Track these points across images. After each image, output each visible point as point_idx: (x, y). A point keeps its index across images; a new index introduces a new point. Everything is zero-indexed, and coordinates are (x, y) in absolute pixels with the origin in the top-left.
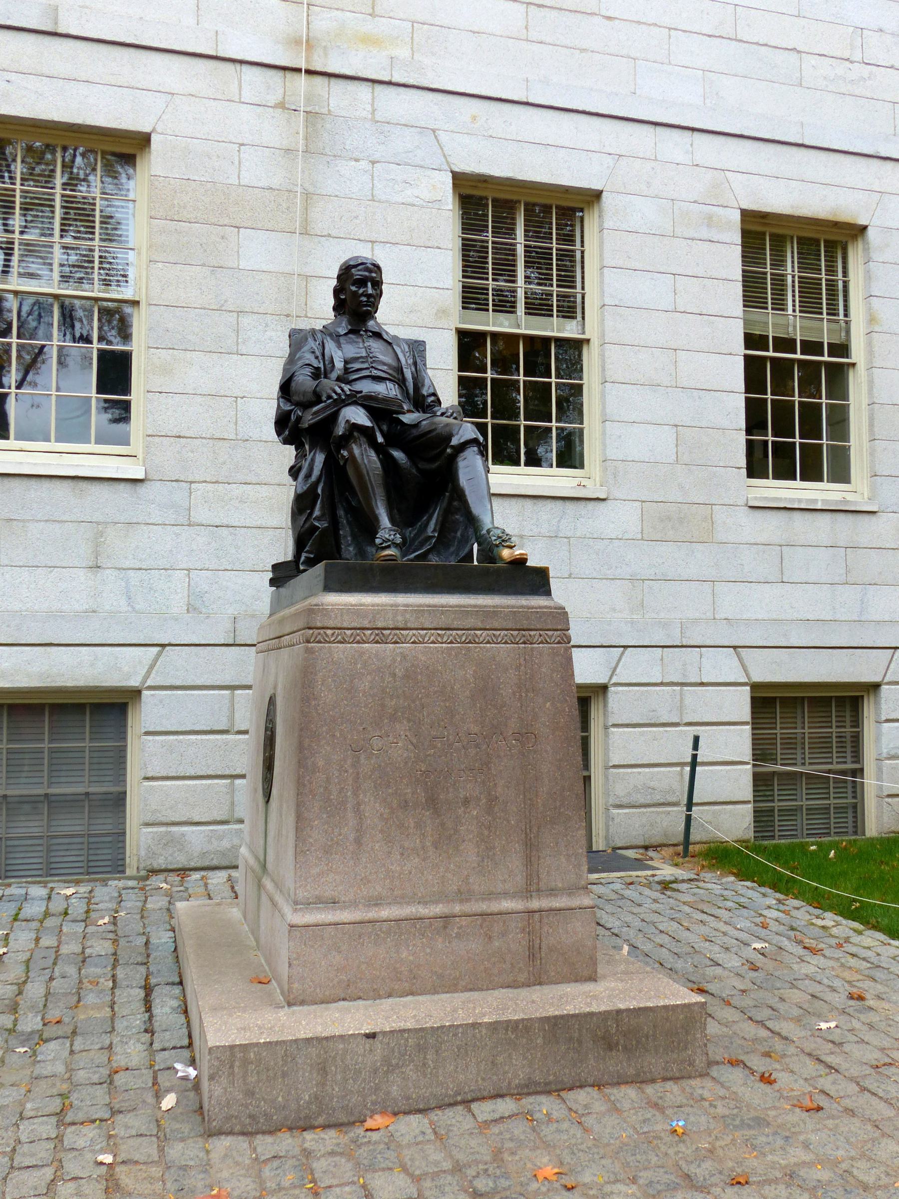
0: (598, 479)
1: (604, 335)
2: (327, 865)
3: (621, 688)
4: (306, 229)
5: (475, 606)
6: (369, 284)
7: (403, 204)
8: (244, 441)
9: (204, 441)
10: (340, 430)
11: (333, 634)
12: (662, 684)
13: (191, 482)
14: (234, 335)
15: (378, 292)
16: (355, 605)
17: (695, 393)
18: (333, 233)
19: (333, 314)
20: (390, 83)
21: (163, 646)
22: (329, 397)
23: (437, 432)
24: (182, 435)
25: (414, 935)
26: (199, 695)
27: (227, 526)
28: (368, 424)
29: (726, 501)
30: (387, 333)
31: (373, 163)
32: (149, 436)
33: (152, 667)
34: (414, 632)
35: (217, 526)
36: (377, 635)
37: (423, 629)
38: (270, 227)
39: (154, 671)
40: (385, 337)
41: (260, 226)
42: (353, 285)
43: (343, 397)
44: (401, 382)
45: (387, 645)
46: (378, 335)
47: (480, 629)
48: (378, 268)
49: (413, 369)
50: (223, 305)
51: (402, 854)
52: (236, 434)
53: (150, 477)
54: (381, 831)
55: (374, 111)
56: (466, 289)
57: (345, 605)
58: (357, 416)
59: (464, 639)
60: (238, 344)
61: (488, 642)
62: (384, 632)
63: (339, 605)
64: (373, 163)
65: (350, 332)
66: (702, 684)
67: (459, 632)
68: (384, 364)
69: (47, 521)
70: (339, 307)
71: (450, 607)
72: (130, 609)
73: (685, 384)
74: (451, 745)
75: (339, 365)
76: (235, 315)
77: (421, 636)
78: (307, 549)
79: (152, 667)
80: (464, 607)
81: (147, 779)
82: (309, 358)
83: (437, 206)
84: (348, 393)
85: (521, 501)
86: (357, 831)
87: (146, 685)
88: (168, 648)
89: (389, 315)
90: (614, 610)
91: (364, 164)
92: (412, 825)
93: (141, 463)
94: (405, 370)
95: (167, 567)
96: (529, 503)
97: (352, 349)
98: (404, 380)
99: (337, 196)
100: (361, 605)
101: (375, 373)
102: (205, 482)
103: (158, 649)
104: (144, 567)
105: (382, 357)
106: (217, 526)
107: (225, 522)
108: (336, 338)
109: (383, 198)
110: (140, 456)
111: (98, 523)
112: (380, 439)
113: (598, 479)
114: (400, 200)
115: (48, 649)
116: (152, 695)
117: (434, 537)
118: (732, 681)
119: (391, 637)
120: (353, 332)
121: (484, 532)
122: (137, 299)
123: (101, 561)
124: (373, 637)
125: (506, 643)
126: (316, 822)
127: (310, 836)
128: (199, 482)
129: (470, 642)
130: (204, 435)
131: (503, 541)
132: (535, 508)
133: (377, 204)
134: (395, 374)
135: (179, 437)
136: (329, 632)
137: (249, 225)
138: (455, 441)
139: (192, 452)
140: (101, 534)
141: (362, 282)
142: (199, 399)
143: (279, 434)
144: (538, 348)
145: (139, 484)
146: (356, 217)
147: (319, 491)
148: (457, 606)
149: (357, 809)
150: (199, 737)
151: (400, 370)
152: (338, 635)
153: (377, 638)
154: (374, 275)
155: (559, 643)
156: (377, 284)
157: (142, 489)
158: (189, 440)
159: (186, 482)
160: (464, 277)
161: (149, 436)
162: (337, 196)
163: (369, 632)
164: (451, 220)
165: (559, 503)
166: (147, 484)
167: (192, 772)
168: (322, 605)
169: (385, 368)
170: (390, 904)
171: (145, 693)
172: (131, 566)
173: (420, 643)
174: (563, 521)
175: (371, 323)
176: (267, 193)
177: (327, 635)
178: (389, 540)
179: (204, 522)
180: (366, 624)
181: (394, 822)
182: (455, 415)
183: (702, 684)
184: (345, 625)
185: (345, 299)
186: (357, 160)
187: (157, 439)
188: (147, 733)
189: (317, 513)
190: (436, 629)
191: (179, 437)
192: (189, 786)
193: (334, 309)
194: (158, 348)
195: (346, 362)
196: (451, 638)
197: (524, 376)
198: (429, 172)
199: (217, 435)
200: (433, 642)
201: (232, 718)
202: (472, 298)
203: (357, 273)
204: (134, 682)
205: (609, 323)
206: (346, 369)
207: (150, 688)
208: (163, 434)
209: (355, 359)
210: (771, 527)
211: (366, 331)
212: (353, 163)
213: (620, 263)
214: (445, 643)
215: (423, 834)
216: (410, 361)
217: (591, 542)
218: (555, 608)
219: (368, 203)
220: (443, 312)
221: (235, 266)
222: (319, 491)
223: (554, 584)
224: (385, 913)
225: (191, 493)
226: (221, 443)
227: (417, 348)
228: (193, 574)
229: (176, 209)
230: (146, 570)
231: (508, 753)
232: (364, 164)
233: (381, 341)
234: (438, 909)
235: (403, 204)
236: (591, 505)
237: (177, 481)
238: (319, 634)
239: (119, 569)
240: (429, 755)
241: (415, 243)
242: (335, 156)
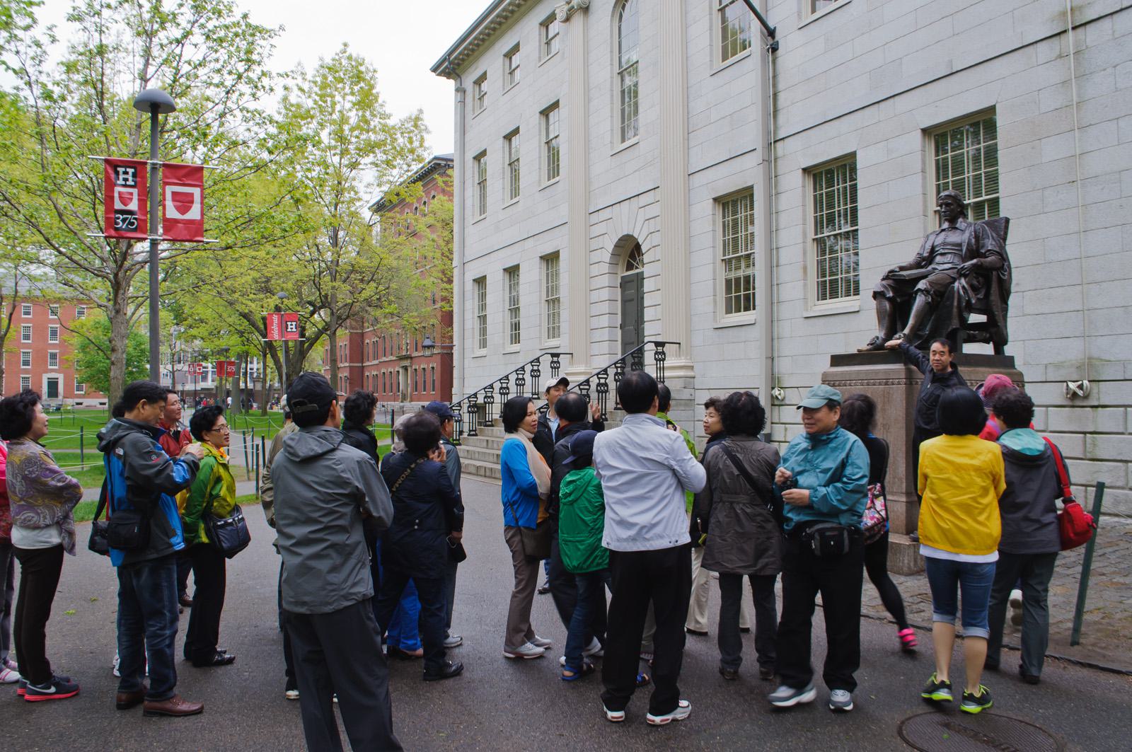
18: (1092, 123)
20: (1121, 10)
31: (1115, 67)
38: (1057, 133)
55: (1114, 32)
64: (1115, 67)
91: (1110, 70)
107: (1041, 312)
146: (1106, 107)
186: (1104, 70)
201: (1047, 424)
232: (1110, 70)
242: (1091, 73)
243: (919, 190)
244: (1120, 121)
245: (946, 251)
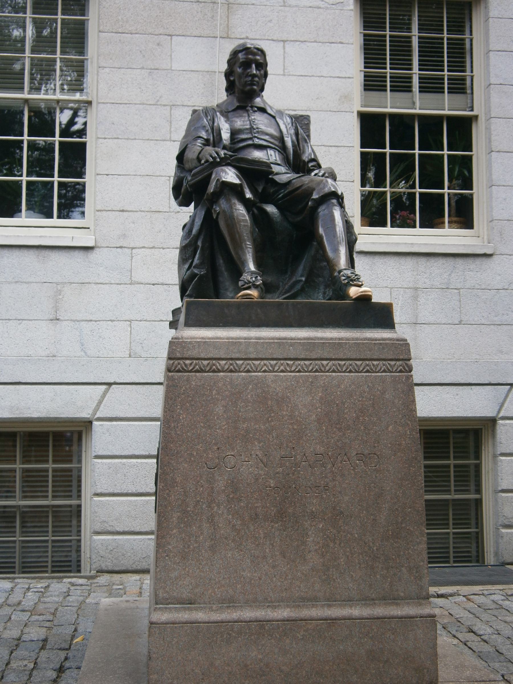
0: (485, 237)
1: (490, 111)
2: (184, 569)
3: (508, 422)
4: (228, 33)
5: (322, 339)
6: (254, 66)
7: (310, 7)
8: (176, 213)
9: (143, 213)
11: (191, 364)
13: (133, 248)
15: (262, 72)
16: (212, 338)
19: (225, 94)
21: (110, 384)
22: (207, 161)
23: (303, 188)
24: (125, 209)
25: (264, 635)
26: (139, 426)
27: (162, 284)
28: (237, 181)
30: (271, 108)
32: (98, 211)
33: (100, 402)
34: (265, 362)
35: (153, 284)
36: (231, 364)
37: (273, 359)
39: (102, 405)
40: (269, 111)
41: (189, 34)
42: (240, 67)
43: (218, 160)
44: (282, 148)
45: (240, 374)
46: (263, 110)
47: (326, 359)
48: (262, 52)
49: (294, 138)
50: (158, 101)
51: (252, 561)
52: (170, 207)
53: (99, 245)
54: (234, 540)
56: (367, 77)
57: (202, 338)
58: (230, 176)
59: (311, 368)
60: (171, 132)
61: (334, 371)
62: (238, 362)
63: (197, 338)
65: (238, 108)
67: (307, 363)
68: (267, 134)
69: (16, 282)
70: (230, 88)
71: (299, 339)
72: (83, 354)
74: (297, 465)
75: (226, 136)
76: (168, 108)
77: (271, 366)
78: (188, 292)
79: (100, 402)
80: (312, 339)
83: (340, 8)
84: (223, 156)
86: (212, 539)
87: (96, 416)
88: (114, 386)
89: (276, 94)
90: (501, 352)
92: (262, 536)
93: (93, 234)
94: (286, 139)
95: (112, 319)
96: (423, 260)
99: (253, 4)
100: (217, 338)
102: (144, 247)
103: (104, 387)
104: (93, 319)
105: (263, 127)
106: (153, 284)
107: (160, 281)
108: (226, 114)
110: (92, 228)
111: (57, 284)
112: (249, 195)
113: (485, 237)
115: (17, 387)
116: (100, 425)
117: (301, 281)
119: (244, 366)
121: (336, 274)
122: (90, 99)
123: (61, 315)
124: (226, 367)
125: (350, 371)
126: (175, 531)
127: (169, 544)
128: (139, 248)
129: (316, 371)
130: (143, 209)
131: (352, 280)
132: (428, 264)
133: (287, 9)
134: (277, 143)
135: (123, 211)
136: (188, 362)
137: (180, 33)
138: (315, 196)
139: (134, 223)
140: (59, 292)
141: (246, 64)
143: (176, 198)
144: (431, 125)
145: (90, 251)
146: (270, 21)
147: (200, 243)
148: (305, 339)
150: (139, 461)
152: (196, 364)
153: (232, 367)
154: (258, 58)
155: (401, 371)
156: (262, 66)
157: (93, 256)
158: (130, 213)
159: (129, 248)
160: (365, 67)
161: (98, 211)
162: (253, 4)
163: (224, 362)
164: (352, 19)
166: (96, 251)
167: (132, 489)
168: (182, 338)
169: (267, 137)
170: (241, 606)
171: (95, 423)
172: (84, 318)
173: (270, 371)
174: (453, 275)
175: (258, 100)
177: (186, 365)
178: (250, 282)
179: (143, 281)
181: (245, 533)
182: (327, 175)
184: (202, 356)
185: (234, 80)
187: (104, 213)
189: (196, 261)
190: (286, 359)
191: (123, 211)
192: (131, 501)
193: (227, 90)
194: (105, 138)
196: (299, 367)
197: (419, 150)
199: (154, 209)
200: (282, 371)
202: (372, 84)
204: (85, 414)
205: (495, 99)
208: (110, 209)
211: (252, 107)
213: (505, 47)
214: (293, 372)
215: (272, 545)
216: (292, 131)
218: (398, 340)
219: (280, 8)
221: (168, 68)
222: (200, 243)
223: (397, 318)
225: (132, 257)
226: (157, 214)
227: (301, 122)
229: (121, 23)
230: (96, 321)
231: (352, 472)
233: (266, 115)
234: (284, 613)
235: (310, 7)
236: (478, 261)
237: (121, 247)
238: (179, 364)
239: (74, 321)
240: (278, 473)
241: (321, 39)
244: (287, 45)
245: (265, 143)
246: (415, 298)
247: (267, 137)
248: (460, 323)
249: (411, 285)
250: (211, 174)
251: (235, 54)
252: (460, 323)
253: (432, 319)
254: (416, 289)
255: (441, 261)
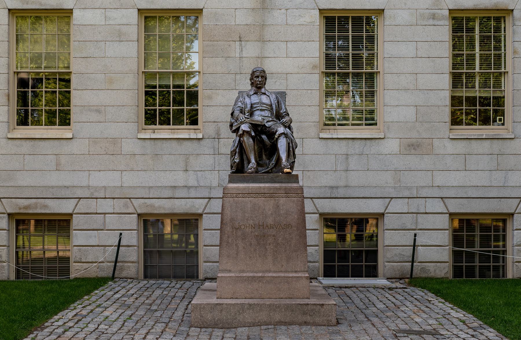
10: (241, 132)
12: (408, 213)
14: (234, 83)
17: (426, 91)
21: (210, 198)
28: (249, 130)
29: (439, 137)
31: (287, 10)
33: (206, 206)
48: (264, 71)
64: (287, 10)
65: (254, 93)
66: (426, 213)
73: (421, 88)
79: (206, 206)
81: (205, 246)
82: (240, 104)
85: (347, 140)
89: (271, 85)
91: (283, 11)
96: (350, 141)
97: (255, 99)
98: (272, 109)
101: (260, 108)
103: (207, 200)
109: (291, 23)
111: (187, 155)
114: (298, 24)
115: (171, 200)
118: (440, 212)
120: (255, 93)
123: (188, 169)
142: (221, 107)
146: (280, 32)
149: (236, 245)
151: (271, 105)
157: (202, 142)
165: (363, 141)
171: (204, 215)
176: (246, 27)
180: (240, 192)
183: (426, 213)
188: (205, 230)
195: (252, 105)
198: (309, 11)
203: (257, 74)
204: (200, 211)
205: (386, 65)
206: (251, 107)
207: (206, 213)
209: (255, 104)
210: (461, 147)
212: (279, 11)
213: (392, 39)
217: (377, 156)
220: (314, 67)
222: (237, 150)
224: (245, 275)
228: (220, 172)
232: (283, 11)
236: (377, 141)
241: (304, 40)
243: (135, 54)
244: (288, 43)
246: (347, 159)
247: (265, 106)
248: (368, 170)
249: (345, 153)
250: (239, 127)
251: (253, 72)
252: (368, 170)
253: (355, 168)
254: (347, 155)
255: (359, 142)
